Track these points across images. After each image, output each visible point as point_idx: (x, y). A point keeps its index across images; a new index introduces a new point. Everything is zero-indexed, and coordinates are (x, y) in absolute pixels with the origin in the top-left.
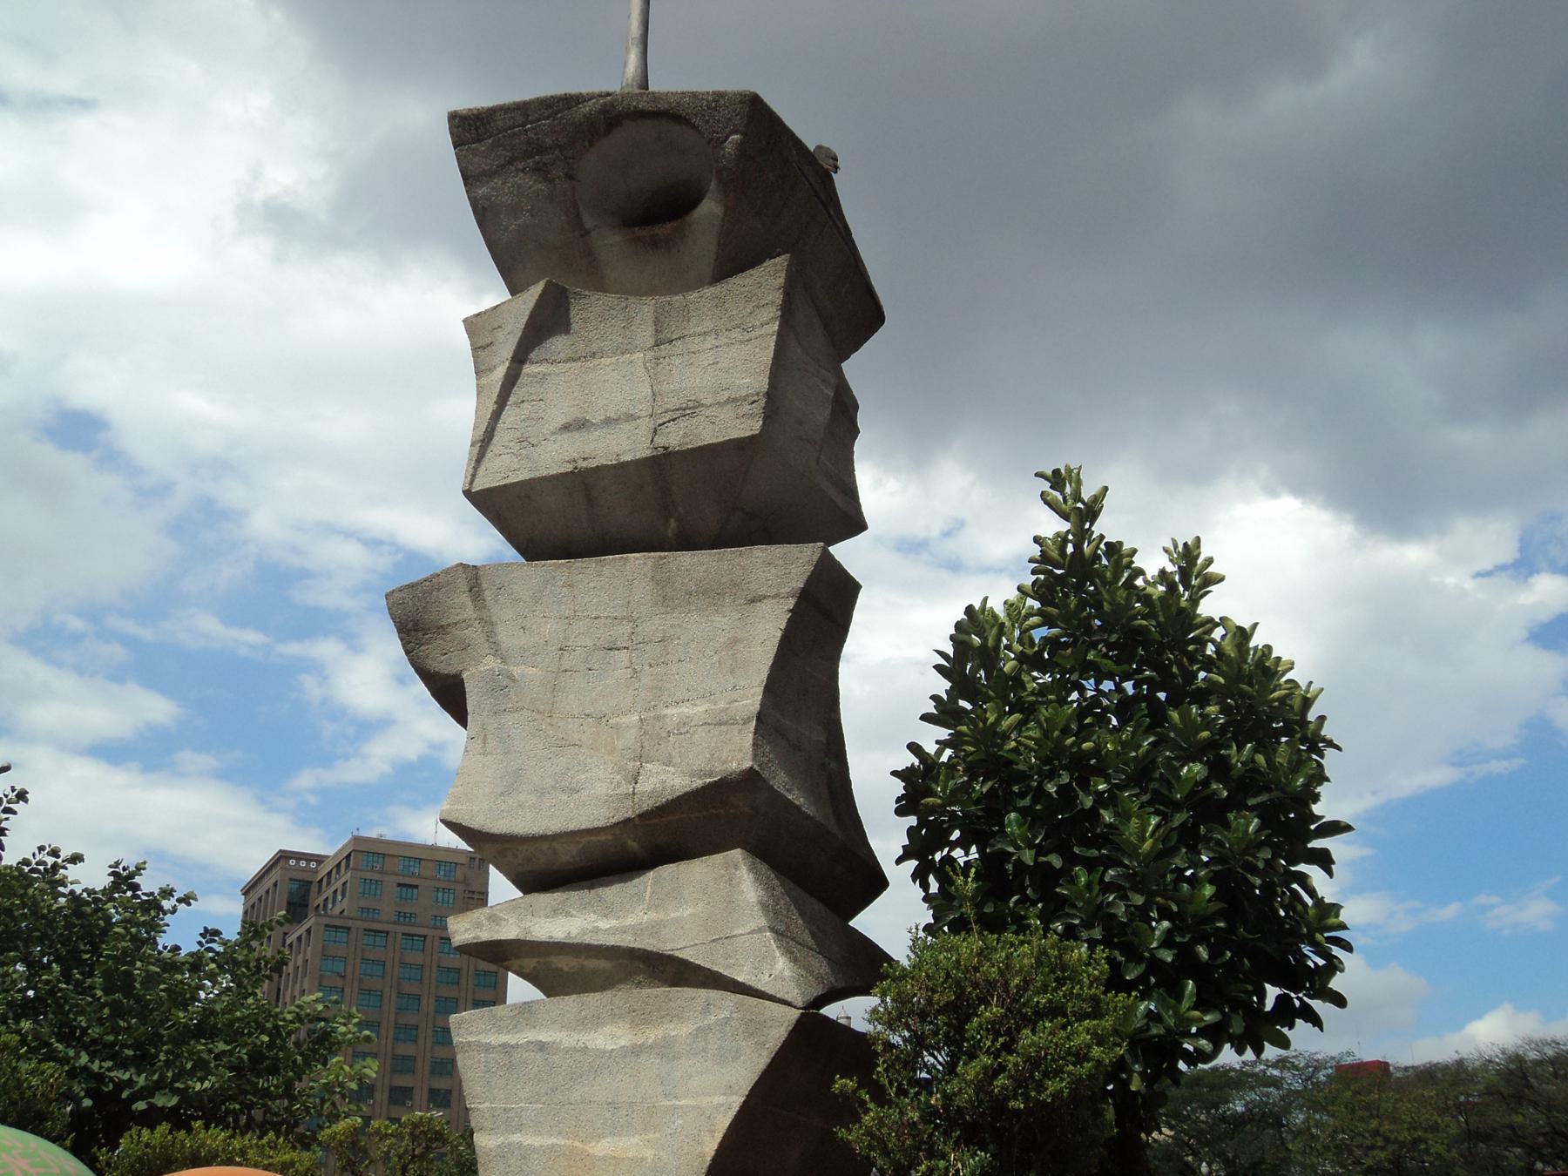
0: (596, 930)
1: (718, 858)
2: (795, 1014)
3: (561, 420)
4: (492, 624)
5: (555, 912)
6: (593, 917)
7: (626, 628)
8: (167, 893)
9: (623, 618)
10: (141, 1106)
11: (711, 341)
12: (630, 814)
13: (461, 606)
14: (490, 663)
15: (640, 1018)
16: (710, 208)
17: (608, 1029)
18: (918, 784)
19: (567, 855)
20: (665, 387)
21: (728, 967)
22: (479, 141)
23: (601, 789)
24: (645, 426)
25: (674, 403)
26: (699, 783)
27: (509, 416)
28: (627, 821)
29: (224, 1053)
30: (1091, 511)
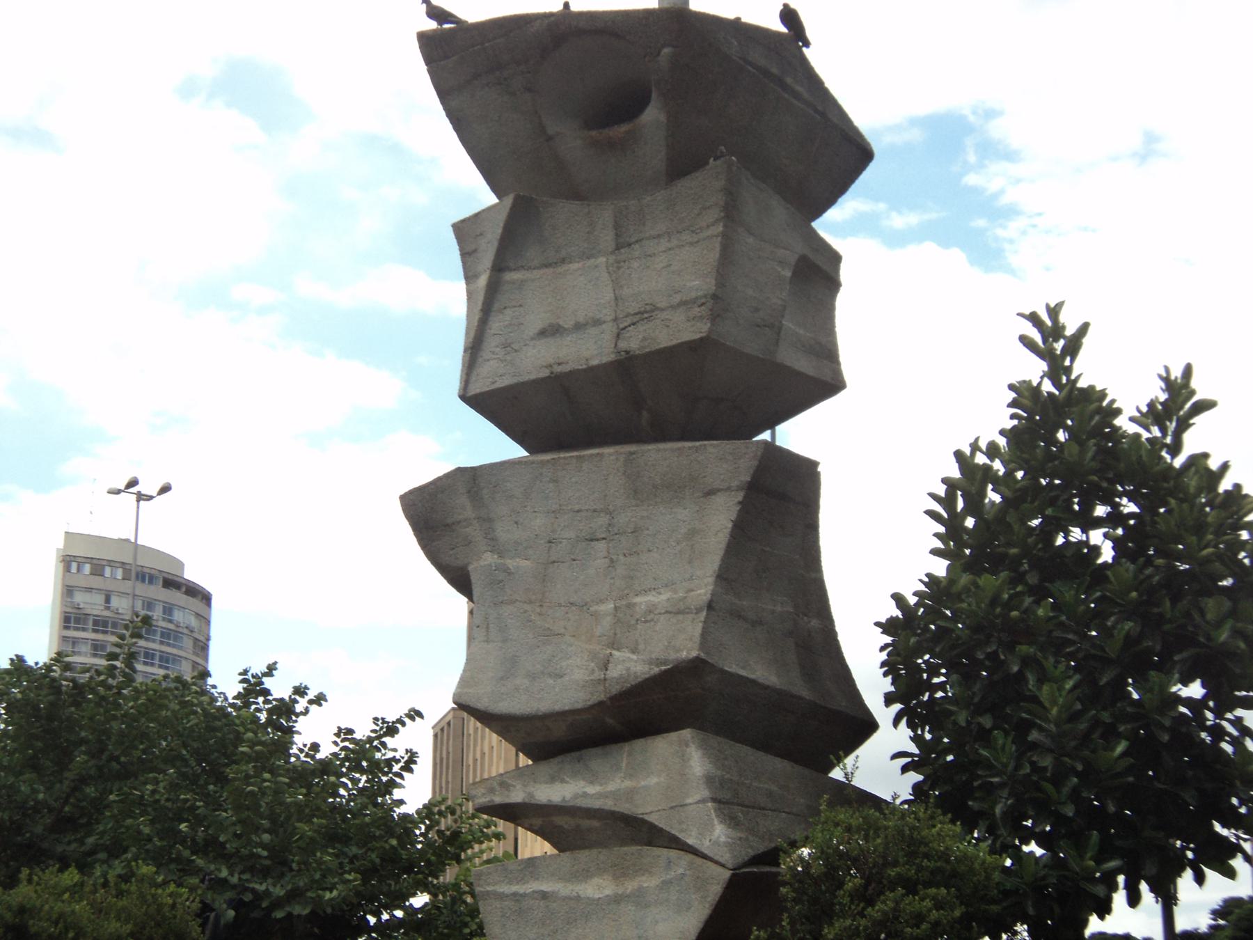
0: (585, 795)
1: (674, 736)
2: (727, 874)
4: (490, 520)
5: (553, 779)
6: (582, 783)
7: (603, 520)
8: (300, 691)
9: (602, 511)
10: (279, 914)
11: (664, 244)
12: (602, 697)
13: (464, 508)
14: (489, 559)
15: (621, 872)
16: (653, 115)
17: (596, 881)
18: (907, 631)
19: (559, 731)
20: (626, 292)
21: (682, 831)
22: (447, 57)
23: (579, 675)
24: (609, 329)
25: (633, 307)
26: (656, 670)
27: (496, 324)
28: (601, 703)
29: (355, 856)
30: (1073, 346)
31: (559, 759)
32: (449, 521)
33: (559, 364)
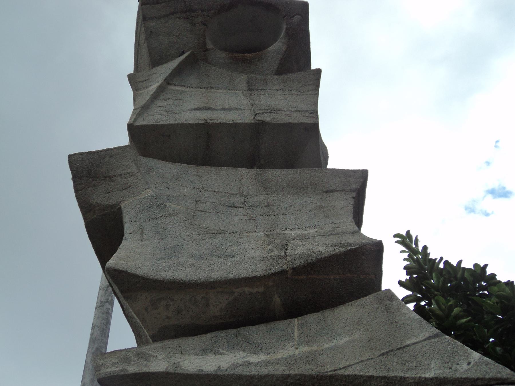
0: (249, 364)
3: (196, 107)
5: (204, 351)
6: (242, 354)
9: (237, 195)
11: (280, 93)
28: (283, 272)
31: (209, 335)
32: (111, 174)
33: (211, 120)
